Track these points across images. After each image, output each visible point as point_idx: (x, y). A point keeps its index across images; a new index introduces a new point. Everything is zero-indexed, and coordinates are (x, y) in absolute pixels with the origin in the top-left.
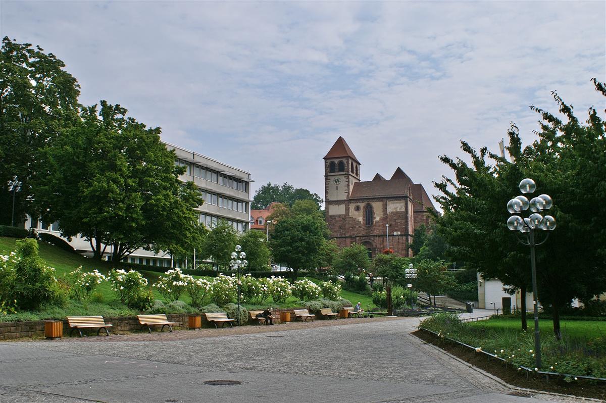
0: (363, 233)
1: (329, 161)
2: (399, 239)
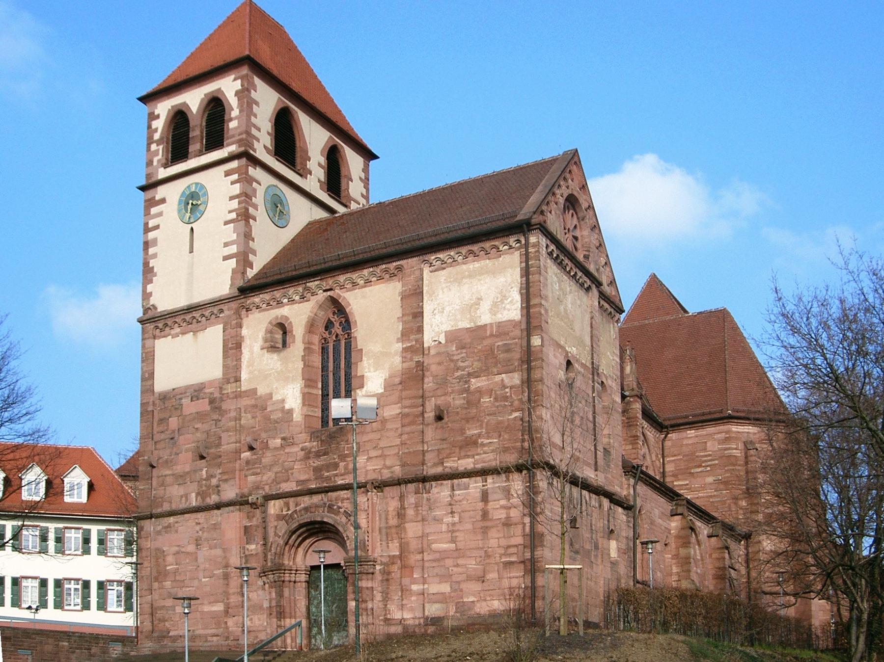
2: (485, 497)
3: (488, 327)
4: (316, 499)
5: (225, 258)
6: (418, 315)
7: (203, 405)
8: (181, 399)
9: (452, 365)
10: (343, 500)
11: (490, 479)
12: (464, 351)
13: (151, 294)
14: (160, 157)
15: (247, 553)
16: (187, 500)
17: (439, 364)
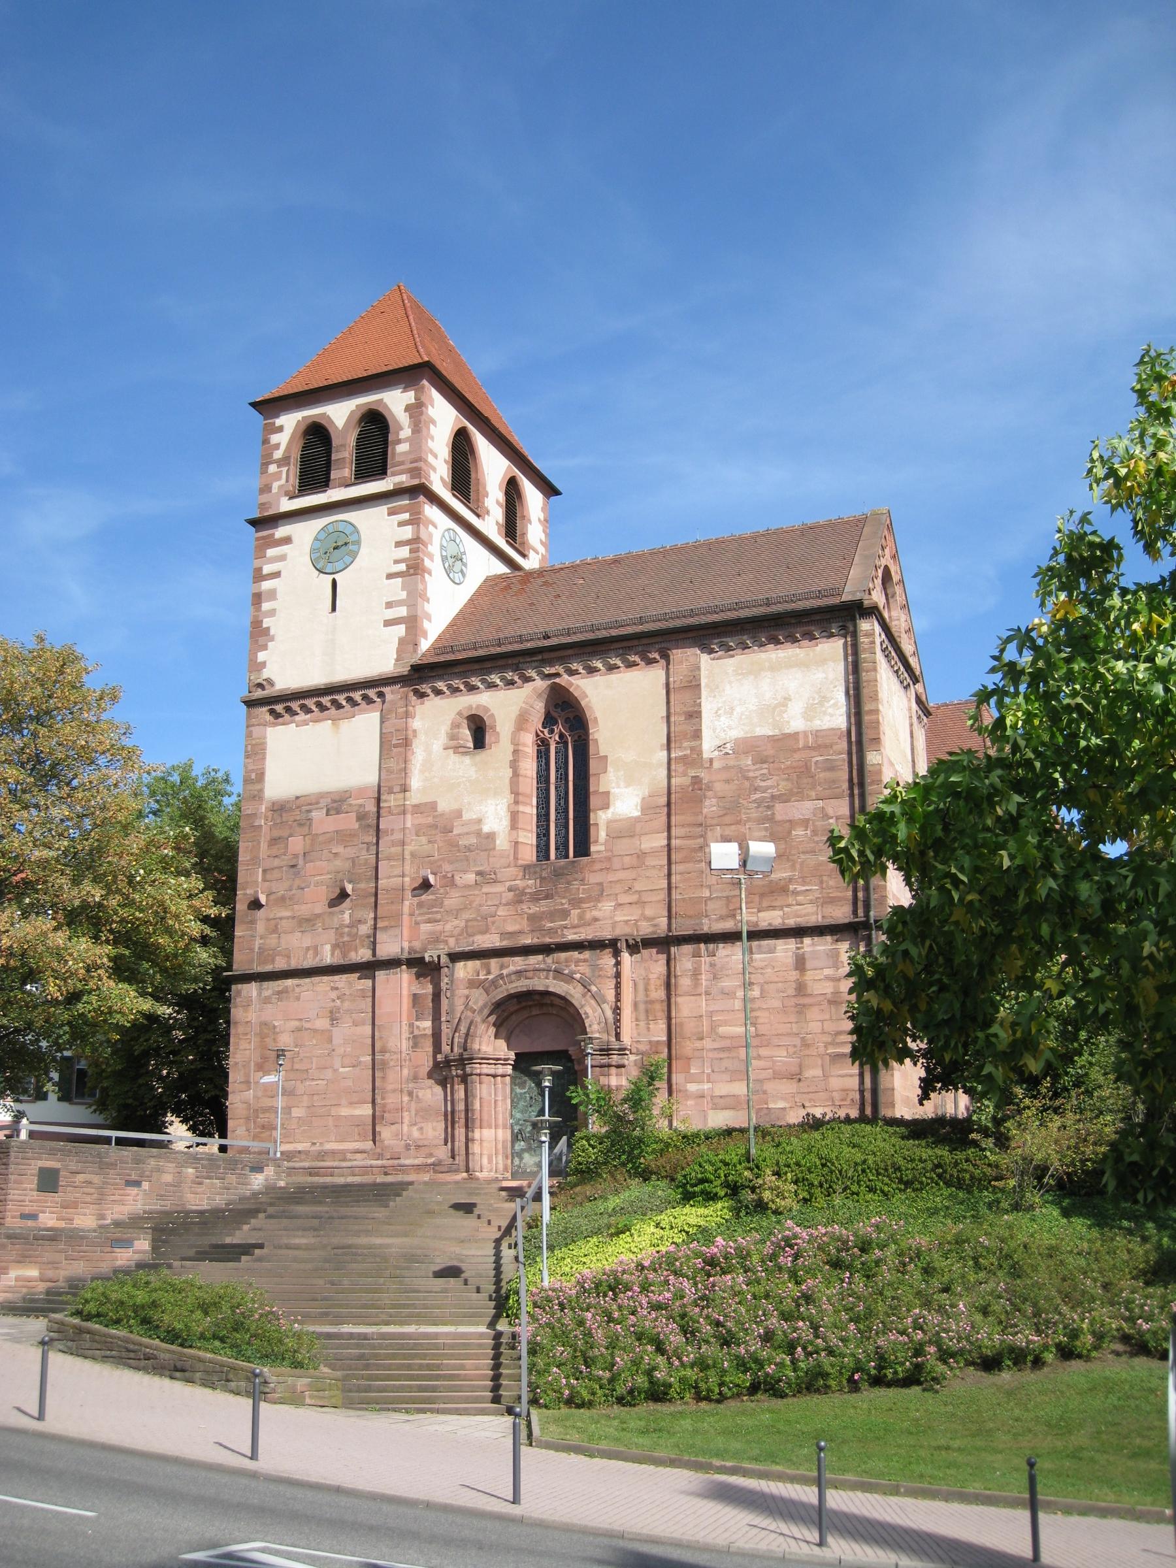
0: (509, 925)
1: (290, 422)
2: (800, 963)
3: (801, 736)
4: (535, 960)
5: (388, 623)
6: (695, 715)
7: (348, 822)
8: (309, 811)
9: (747, 784)
10: (577, 962)
11: (807, 941)
12: (765, 766)
13: (264, 664)
14: (283, 481)
15: (416, 1032)
16: (316, 953)
17: (727, 781)
